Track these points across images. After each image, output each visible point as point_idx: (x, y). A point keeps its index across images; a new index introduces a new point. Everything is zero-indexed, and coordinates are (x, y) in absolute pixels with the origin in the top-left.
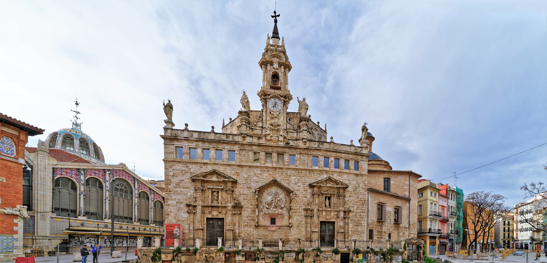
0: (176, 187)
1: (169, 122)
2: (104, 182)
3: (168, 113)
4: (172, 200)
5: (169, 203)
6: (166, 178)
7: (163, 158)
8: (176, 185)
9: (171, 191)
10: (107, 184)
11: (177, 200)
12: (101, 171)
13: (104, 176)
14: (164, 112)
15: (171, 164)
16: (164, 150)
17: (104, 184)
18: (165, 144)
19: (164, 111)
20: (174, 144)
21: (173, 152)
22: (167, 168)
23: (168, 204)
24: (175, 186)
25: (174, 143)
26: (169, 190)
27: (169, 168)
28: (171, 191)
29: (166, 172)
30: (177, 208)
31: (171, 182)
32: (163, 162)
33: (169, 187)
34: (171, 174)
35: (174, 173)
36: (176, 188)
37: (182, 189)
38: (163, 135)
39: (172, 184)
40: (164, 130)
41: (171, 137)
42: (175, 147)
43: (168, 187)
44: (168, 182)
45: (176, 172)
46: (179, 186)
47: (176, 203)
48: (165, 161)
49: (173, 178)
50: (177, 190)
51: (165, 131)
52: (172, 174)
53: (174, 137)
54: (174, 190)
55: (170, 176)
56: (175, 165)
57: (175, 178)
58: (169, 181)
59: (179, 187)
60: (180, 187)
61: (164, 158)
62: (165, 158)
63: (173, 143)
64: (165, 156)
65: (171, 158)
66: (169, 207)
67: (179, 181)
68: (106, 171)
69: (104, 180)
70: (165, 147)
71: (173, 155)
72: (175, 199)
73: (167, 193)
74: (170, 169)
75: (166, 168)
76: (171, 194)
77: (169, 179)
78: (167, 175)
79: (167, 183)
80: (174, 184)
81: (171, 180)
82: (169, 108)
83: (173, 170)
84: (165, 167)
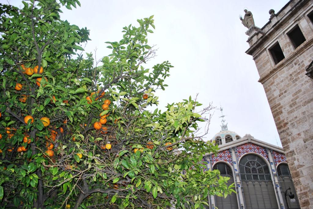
0: (291, 112)
1: (252, 29)
2: (232, 165)
3: (247, 23)
4: (293, 139)
5: (291, 149)
6: (272, 105)
7: (258, 78)
8: (291, 106)
9: (287, 123)
10: (236, 166)
11: (303, 135)
12: (226, 152)
13: (230, 157)
14: (244, 26)
15: (271, 79)
16: (257, 66)
17: (231, 166)
18: (254, 59)
19: (244, 25)
20: (266, 49)
21: (268, 60)
22: (268, 88)
23: (291, 152)
24: (290, 109)
25: (265, 47)
26: (282, 124)
27: (271, 87)
28: (287, 123)
29: (269, 97)
30: (310, 152)
31: (281, 107)
32: (260, 83)
33: (282, 119)
34: (276, 93)
35: (281, 88)
36: (292, 114)
37: (304, 109)
38: (249, 47)
39: (283, 111)
40: (249, 43)
41: (258, 43)
42: (268, 51)
43: (279, 119)
44: (277, 110)
45: (282, 84)
46: (296, 106)
47: (302, 142)
48: (262, 81)
49: (281, 99)
50: (295, 116)
51: (250, 44)
52: (279, 93)
53: (261, 40)
54: (291, 118)
55: (276, 98)
56: (277, 76)
57: (285, 96)
58: (277, 108)
59: (296, 108)
60: (298, 106)
61: (259, 78)
62: (261, 76)
63: (263, 49)
64: (259, 74)
65: (268, 70)
66: (294, 156)
67: (293, 98)
68: (231, 151)
69: (231, 163)
70: (256, 63)
71: (269, 64)
72: (299, 134)
73: (282, 129)
74: (273, 88)
75: (267, 90)
76: (288, 128)
77: (277, 103)
78: (271, 101)
79: (276, 113)
80: (288, 108)
81: (279, 104)
82: (247, 17)
83: (277, 84)
84: (265, 89)
